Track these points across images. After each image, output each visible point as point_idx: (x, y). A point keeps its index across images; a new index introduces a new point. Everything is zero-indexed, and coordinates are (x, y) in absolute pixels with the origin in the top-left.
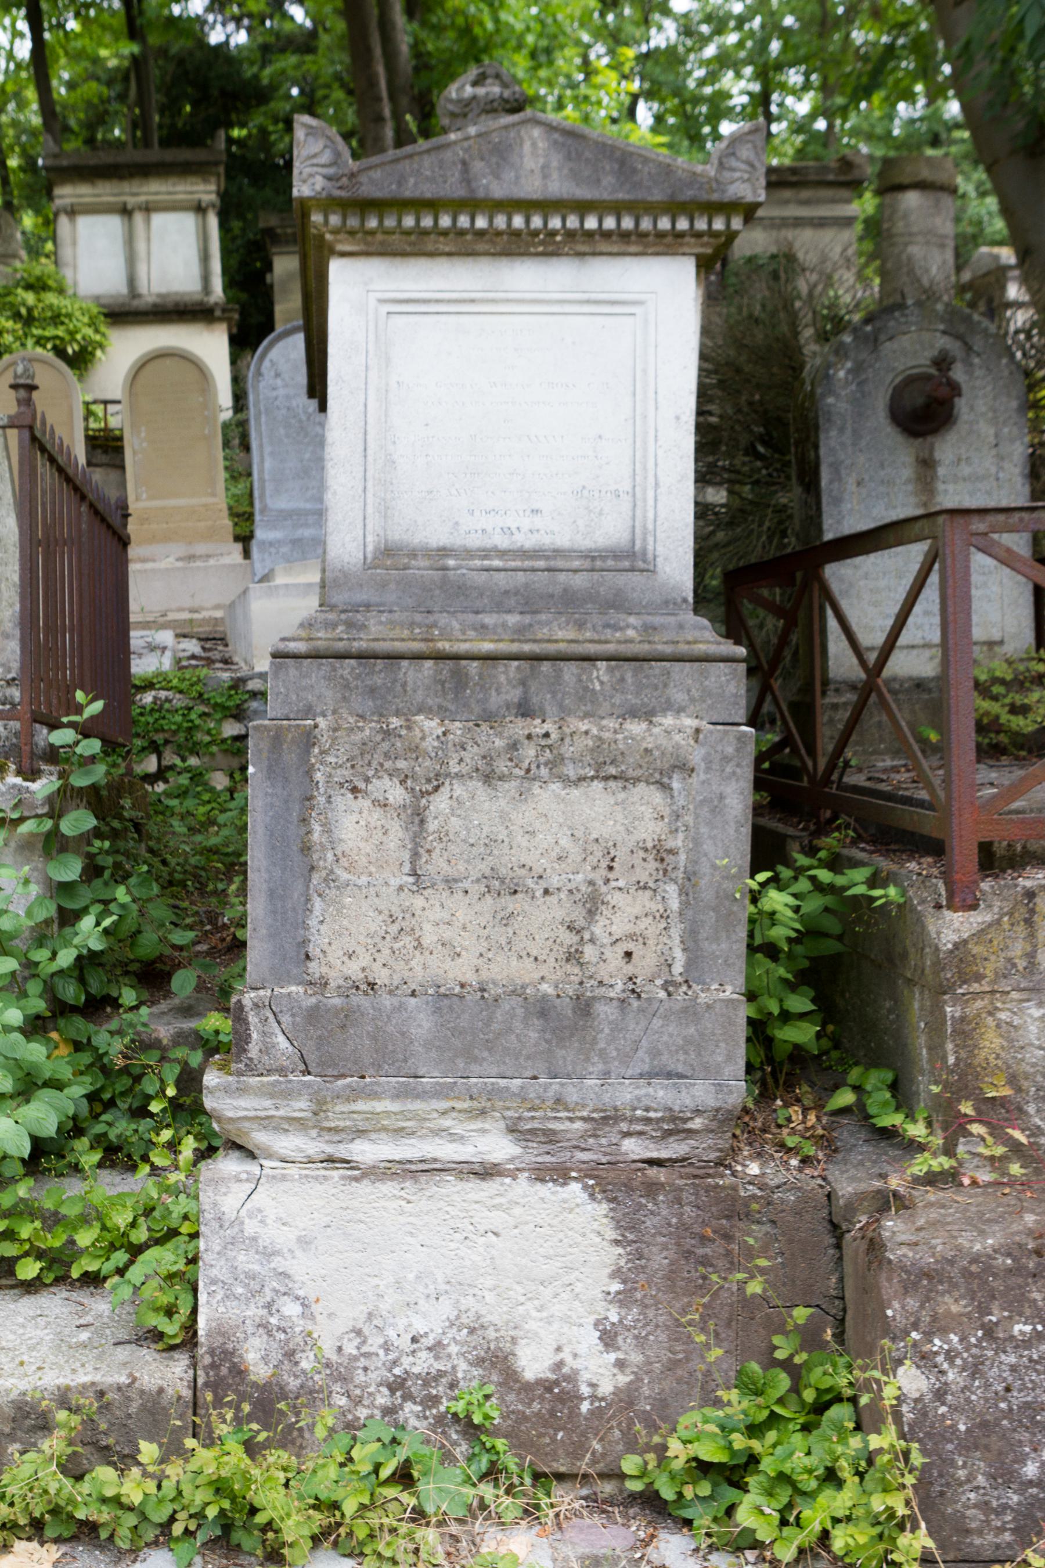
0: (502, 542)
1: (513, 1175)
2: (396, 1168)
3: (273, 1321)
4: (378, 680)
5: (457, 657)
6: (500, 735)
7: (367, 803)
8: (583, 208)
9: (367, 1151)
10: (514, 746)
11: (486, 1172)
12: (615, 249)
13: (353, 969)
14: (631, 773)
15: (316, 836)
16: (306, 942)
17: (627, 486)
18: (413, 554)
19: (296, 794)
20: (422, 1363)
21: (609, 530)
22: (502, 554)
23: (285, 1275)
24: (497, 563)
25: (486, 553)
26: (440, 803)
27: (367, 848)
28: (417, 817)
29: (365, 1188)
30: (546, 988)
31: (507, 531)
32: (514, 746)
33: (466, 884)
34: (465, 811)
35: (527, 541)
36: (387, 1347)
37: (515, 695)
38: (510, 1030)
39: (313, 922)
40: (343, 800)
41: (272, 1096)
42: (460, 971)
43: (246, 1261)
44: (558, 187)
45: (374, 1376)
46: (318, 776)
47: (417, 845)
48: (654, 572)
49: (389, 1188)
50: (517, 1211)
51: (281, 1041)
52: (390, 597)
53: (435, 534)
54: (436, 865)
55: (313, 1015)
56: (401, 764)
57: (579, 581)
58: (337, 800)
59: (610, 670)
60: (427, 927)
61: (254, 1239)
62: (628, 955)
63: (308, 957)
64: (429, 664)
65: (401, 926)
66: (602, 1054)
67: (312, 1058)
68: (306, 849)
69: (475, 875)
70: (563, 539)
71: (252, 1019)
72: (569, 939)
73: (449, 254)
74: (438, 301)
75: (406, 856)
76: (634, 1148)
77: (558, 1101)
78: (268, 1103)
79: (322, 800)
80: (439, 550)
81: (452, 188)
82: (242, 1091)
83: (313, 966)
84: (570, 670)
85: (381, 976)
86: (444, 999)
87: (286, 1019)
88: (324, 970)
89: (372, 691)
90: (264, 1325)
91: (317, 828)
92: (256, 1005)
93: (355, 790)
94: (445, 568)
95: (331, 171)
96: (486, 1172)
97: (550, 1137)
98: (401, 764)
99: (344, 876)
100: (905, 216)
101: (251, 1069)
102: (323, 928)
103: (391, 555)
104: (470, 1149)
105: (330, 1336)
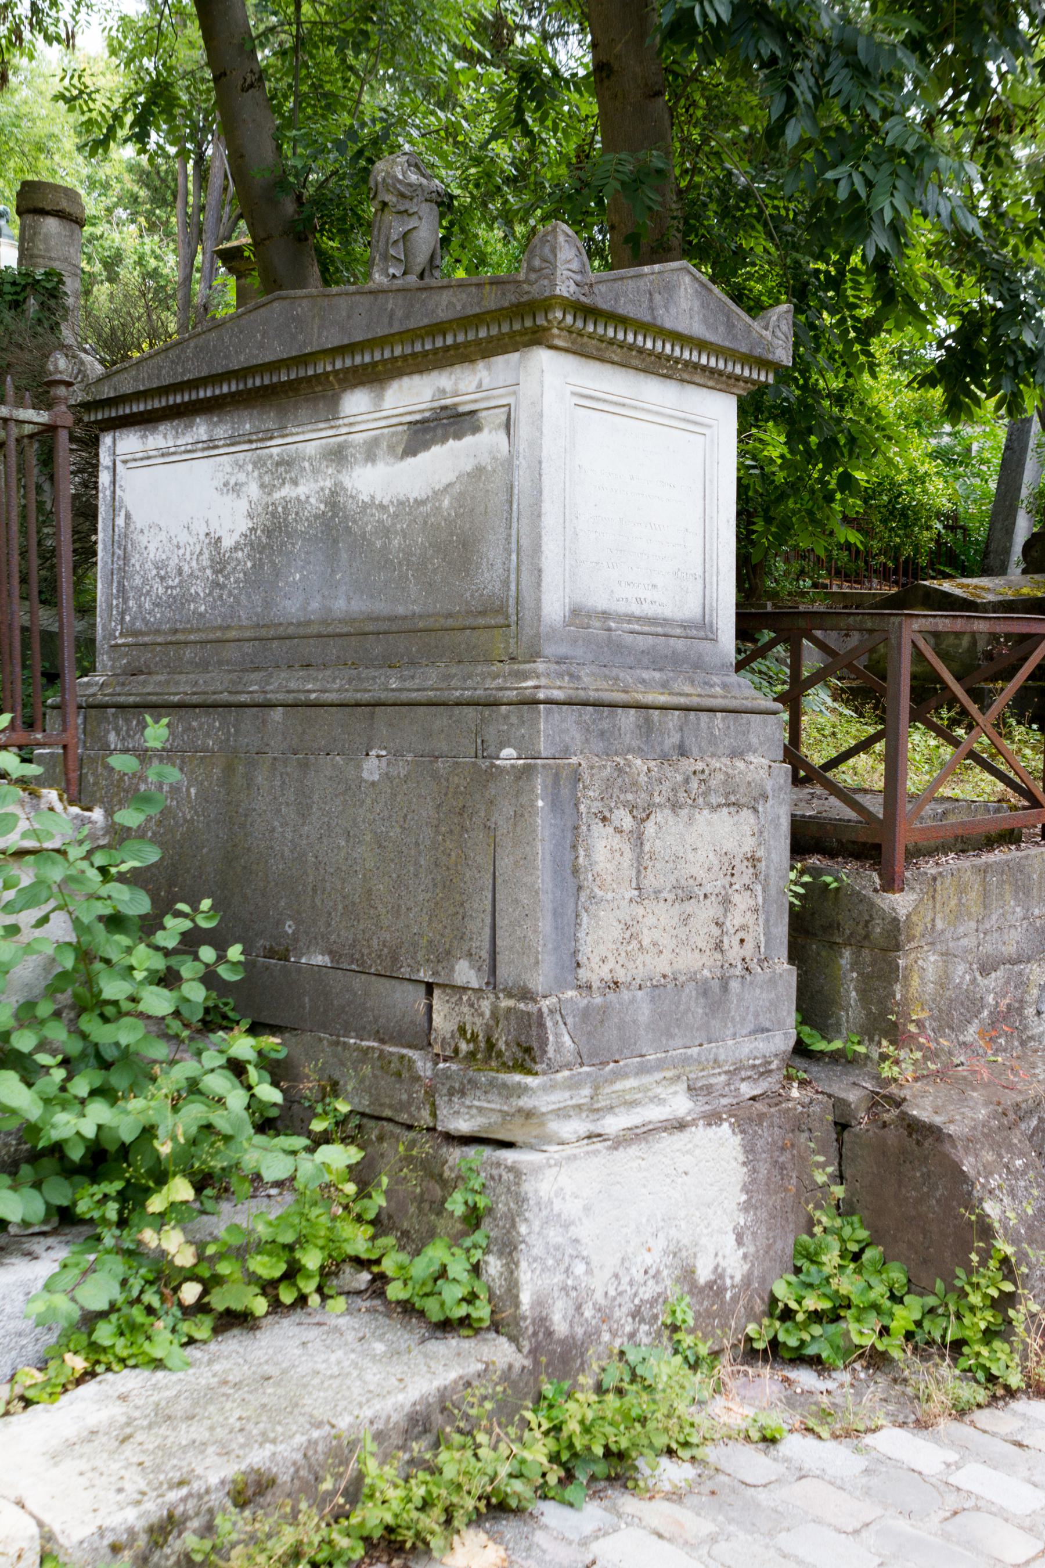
0: (636, 609)
1: (694, 1123)
2: (630, 1135)
3: (570, 1282)
4: (605, 725)
5: (647, 707)
6: (677, 771)
7: (611, 830)
8: (717, 350)
9: (613, 1124)
10: (687, 781)
11: (681, 1126)
12: (711, 383)
13: (604, 972)
14: (742, 801)
15: (581, 860)
16: (576, 952)
17: (700, 572)
18: (589, 616)
19: (569, 824)
20: (647, 1292)
21: (689, 608)
22: (639, 619)
23: (576, 1241)
24: (637, 627)
25: (631, 618)
26: (650, 828)
27: (611, 867)
28: (638, 839)
29: (620, 1154)
30: (706, 973)
31: (640, 601)
32: (687, 781)
33: (665, 895)
34: (665, 831)
35: (649, 610)
36: (631, 1284)
37: (676, 739)
38: (688, 1009)
39: (581, 935)
40: (598, 828)
41: (570, 1088)
42: (662, 965)
43: (554, 1235)
44: (697, 328)
45: (624, 1310)
46: (582, 808)
47: (640, 864)
48: (716, 640)
49: (633, 1150)
50: (697, 1152)
51: (566, 1039)
52: (579, 652)
53: (599, 601)
54: (650, 881)
55: (586, 1014)
56: (630, 797)
57: (680, 645)
58: (593, 827)
59: (723, 719)
60: (645, 931)
61: (559, 1215)
62: (742, 941)
63: (578, 965)
64: (633, 711)
65: (631, 932)
66: (733, 1019)
67: (584, 1052)
68: (576, 871)
69: (669, 887)
70: (668, 611)
71: (549, 1024)
72: (716, 931)
73: (613, 363)
74: (605, 401)
75: (634, 873)
76: (747, 1090)
77: (716, 1061)
78: (567, 1094)
79: (584, 828)
80: (604, 613)
81: (637, 311)
82: (553, 1087)
83: (581, 971)
84: (704, 716)
85: (621, 976)
86: (660, 987)
87: (570, 1020)
88: (589, 974)
89: (602, 733)
90: (564, 1289)
91: (582, 853)
92: (551, 1011)
93: (604, 819)
94: (609, 629)
95: (578, 278)
96: (681, 1126)
97: (708, 1089)
98: (630, 797)
99: (599, 893)
100: (46, 240)
101: (553, 1069)
102: (589, 939)
103: (577, 614)
104: (668, 1109)
105: (600, 1285)
